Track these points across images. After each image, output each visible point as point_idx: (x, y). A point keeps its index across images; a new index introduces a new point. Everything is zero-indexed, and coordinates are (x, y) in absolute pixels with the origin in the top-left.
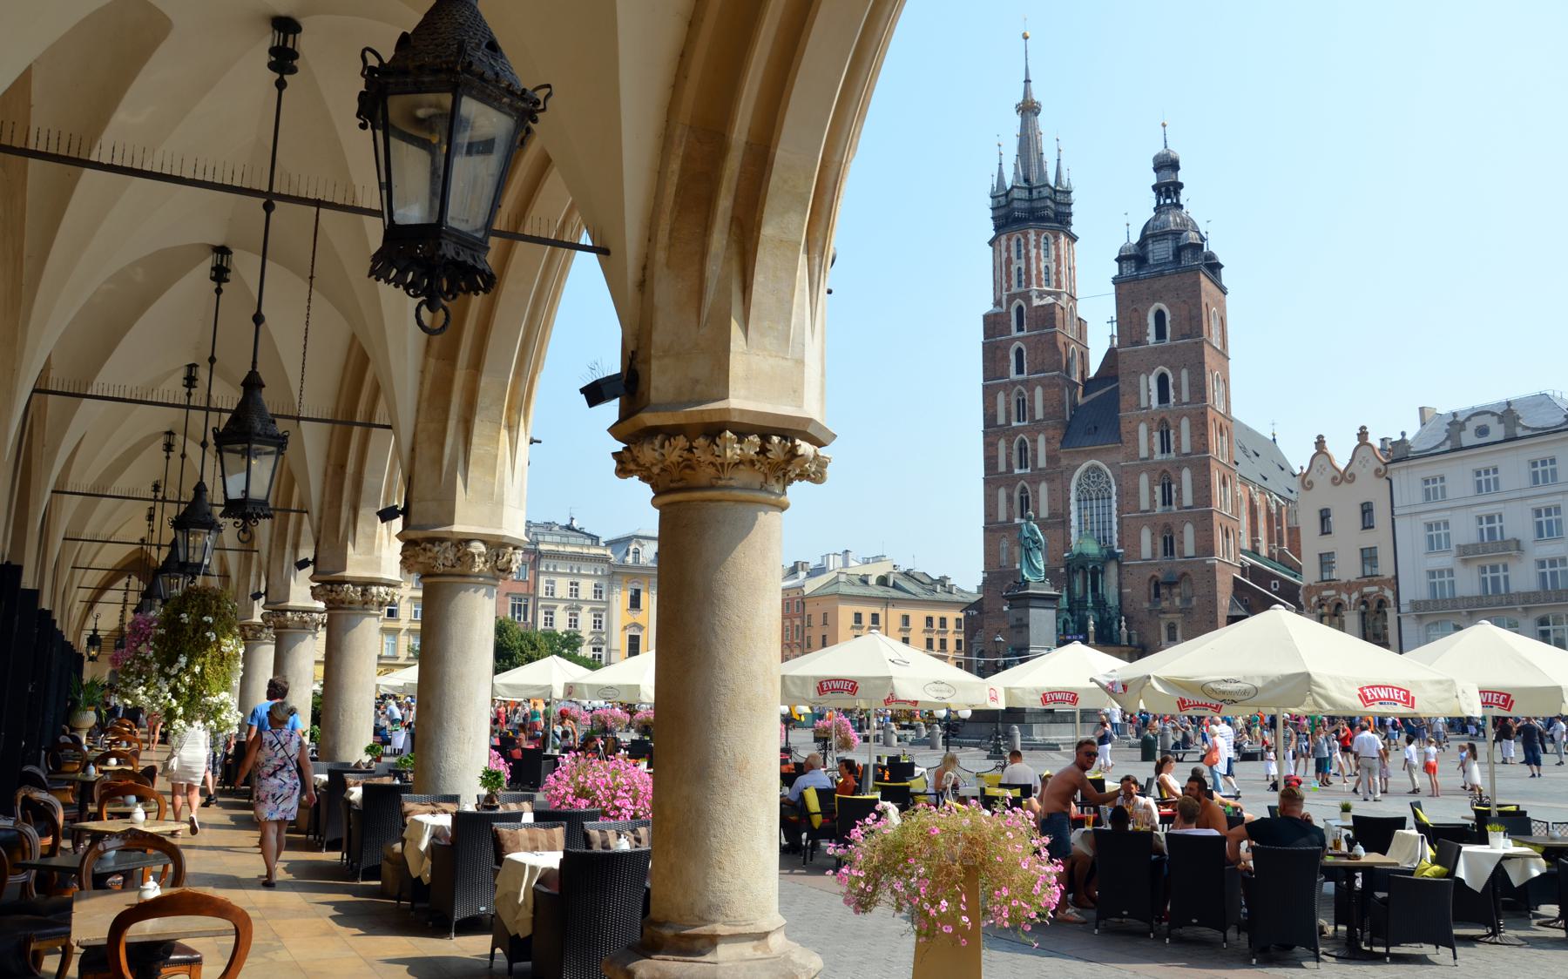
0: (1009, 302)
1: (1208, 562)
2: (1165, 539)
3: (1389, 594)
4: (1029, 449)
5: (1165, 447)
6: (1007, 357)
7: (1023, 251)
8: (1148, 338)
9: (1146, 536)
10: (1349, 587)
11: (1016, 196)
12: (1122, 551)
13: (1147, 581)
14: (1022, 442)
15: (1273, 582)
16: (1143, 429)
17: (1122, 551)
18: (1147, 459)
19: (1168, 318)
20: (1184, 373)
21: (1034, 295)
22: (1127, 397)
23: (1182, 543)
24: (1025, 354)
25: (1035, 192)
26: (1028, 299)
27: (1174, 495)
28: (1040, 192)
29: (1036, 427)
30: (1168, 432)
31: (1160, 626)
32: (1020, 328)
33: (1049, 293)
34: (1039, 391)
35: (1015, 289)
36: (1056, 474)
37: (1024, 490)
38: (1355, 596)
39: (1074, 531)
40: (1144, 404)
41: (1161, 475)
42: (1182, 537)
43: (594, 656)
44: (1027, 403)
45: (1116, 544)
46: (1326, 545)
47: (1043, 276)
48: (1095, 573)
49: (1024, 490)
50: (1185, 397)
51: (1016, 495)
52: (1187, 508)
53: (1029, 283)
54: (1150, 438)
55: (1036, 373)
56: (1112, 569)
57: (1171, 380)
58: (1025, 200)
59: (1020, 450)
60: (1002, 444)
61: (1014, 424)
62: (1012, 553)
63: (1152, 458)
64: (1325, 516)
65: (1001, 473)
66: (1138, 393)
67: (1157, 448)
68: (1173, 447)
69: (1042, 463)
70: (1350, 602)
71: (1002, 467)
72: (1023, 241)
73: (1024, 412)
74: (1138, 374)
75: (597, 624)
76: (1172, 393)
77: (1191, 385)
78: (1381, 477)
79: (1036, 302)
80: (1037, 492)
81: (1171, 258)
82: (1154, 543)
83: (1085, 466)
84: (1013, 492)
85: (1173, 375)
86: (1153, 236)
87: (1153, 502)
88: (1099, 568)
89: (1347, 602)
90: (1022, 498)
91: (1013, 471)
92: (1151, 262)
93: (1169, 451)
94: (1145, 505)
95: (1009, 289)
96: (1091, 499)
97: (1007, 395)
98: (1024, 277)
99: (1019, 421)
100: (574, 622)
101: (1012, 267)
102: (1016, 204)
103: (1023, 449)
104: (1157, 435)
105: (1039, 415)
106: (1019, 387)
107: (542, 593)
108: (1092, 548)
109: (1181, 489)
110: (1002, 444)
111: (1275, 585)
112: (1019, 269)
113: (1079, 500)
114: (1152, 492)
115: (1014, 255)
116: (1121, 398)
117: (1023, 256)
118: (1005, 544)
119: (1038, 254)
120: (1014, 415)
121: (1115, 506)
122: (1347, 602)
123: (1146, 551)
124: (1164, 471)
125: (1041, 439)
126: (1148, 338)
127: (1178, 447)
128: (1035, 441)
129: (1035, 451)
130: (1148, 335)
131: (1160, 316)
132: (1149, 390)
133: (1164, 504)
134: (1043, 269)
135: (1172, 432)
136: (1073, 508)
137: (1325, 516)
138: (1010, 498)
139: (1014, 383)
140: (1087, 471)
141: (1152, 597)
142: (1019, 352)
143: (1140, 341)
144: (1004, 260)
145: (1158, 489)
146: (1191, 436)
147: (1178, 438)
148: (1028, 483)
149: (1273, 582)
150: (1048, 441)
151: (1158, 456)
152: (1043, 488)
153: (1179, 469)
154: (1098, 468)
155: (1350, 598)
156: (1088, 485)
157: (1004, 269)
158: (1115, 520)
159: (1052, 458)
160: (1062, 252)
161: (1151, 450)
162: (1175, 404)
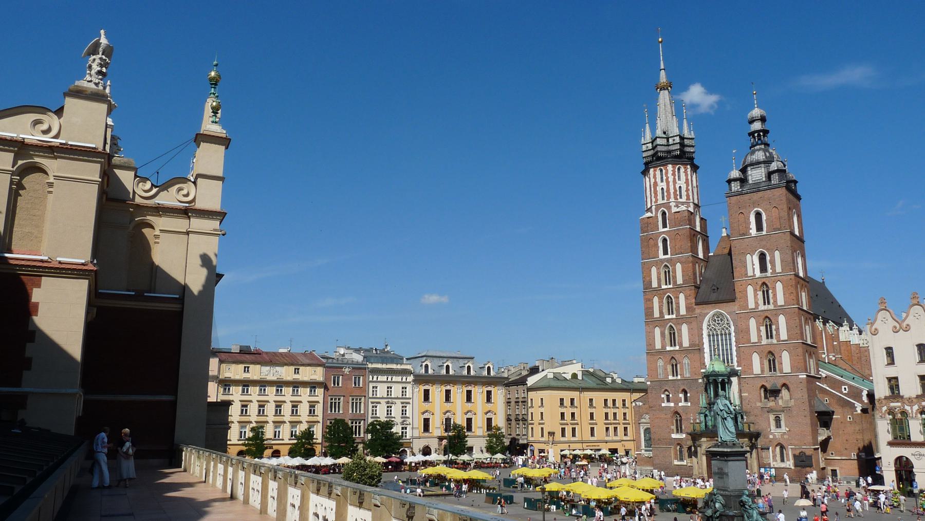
0: (657, 210)
1: (800, 376)
2: (770, 361)
4: (674, 303)
5: (766, 301)
6: (656, 245)
7: (664, 178)
8: (751, 231)
9: (756, 359)
10: (910, 401)
11: (658, 143)
12: (740, 368)
13: (759, 388)
15: (843, 387)
16: (750, 290)
17: (740, 368)
18: (754, 309)
19: (764, 217)
20: (777, 254)
21: (673, 204)
23: (782, 363)
24: (668, 243)
25: (671, 140)
26: (669, 208)
27: (774, 333)
28: (674, 140)
29: (678, 288)
30: (767, 291)
31: (769, 418)
32: (665, 226)
33: (683, 203)
34: (679, 267)
35: (660, 201)
36: (693, 320)
38: (916, 407)
39: (707, 356)
40: (750, 273)
41: (764, 319)
43: (402, 432)
44: (671, 273)
45: (735, 364)
46: (892, 372)
47: (678, 193)
48: (723, 384)
50: (779, 269)
51: (667, 332)
52: (783, 341)
53: (669, 198)
54: (756, 296)
56: (734, 380)
57: (768, 258)
58: (665, 145)
60: (656, 300)
61: (664, 287)
62: (666, 369)
63: (758, 309)
64: (889, 351)
65: (656, 318)
66: (746, 267)
67: (761, 301)
68: (771, 301)
69: (683, 311)
70: (912, 411)
71: (657, 314)
72: (664, 171)
73: (669, 279)
74: (745, 254)
75: (404, 412)
76: (769, 266)
77: (782, 261)
79: (674, 210)
80: (681, 330)
81: (764, 179)
82: (762, 364)
83: (712, 313)
84: (665, 330)
85: (770, 255)
86: (752, 164)
87: (760, 337)
88: (726, 380)
89: (910, 411)
90: (670, 333)
91: (664, 317)
92: (750, 182)
93: (769, 303)
94: (754, 338)
95: (656, 201)
97: (658, 269)
98: (665, 194)
99: (666, 284)
100: (389, 412)
101: (658, 187)
102: (659, 148)
104: (760, 294)
105: (680, 281)
107: (371, 395)
108: (719, 367)
109: (779, 328)
110: (656, 300)
111: (845, 388)
112: (662, 189)
113: (709, 336)
114: (759, 331)
115: (658, 180)
117: (664, 181)
118: (660, 363)
119: (674, 179)
120: (663, 281)
121: (733, 339)
123: (757, 369)
124: (767, 317)
125: (682, 296)
126: (751, 231)
127: (775, 301)
128: (677, 298)
129: (678, 304)
130: (751, 229)
131: (758, 216)
132: (753, 265)
133: (767, 338)
134: (678, 189)
135: (770, 291)
137: (889, 351)
138: (663, 334)
139: (662, 261)
141: (763, 399)
142: (665, 240)
143: (746, 232)
144: (652, 184)
145: (763, 329)
146: (784, 294)
147: (775, 295)
148: (674, 324)
149: (843, 387)
150: (686, 298)
151: (762, 307)
152: (685, 328)
153: (777, 315)
154: (721, 314)
155: (912, 409)
156: (714, 325)
157: (652, 189)
158: (734, 348)
159: (688, 308)
160: (689, 177)
161: (757, 303)
162: (772, 273)
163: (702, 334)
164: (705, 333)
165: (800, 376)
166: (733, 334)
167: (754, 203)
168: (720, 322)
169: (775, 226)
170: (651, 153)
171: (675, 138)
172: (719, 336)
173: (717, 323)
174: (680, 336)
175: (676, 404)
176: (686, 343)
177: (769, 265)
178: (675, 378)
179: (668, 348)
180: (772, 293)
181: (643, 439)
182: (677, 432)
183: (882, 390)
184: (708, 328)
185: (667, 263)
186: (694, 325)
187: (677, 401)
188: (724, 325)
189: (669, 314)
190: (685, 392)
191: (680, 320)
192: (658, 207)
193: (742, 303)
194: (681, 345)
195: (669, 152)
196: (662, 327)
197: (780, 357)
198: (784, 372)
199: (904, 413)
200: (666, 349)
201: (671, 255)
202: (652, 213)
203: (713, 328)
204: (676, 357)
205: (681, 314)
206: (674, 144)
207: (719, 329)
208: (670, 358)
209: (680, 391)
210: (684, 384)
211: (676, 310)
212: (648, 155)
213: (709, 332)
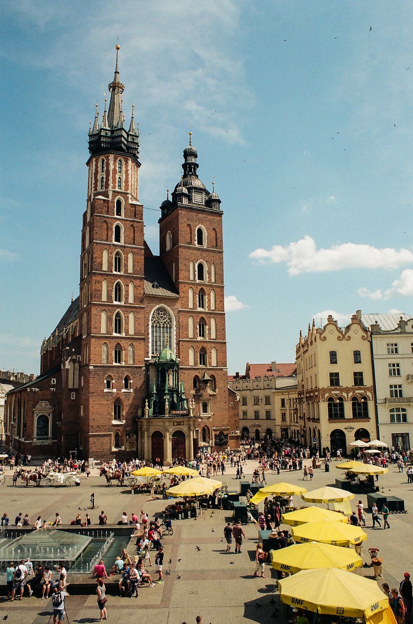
2: (200, 355)
3: (369, 394)
9: (191, 353)
14: (118, 284)
22: (183, 272)
23: (211, 358)
24: (122, 231)
37: (118, 315)
42: (211, 355)
49: (118, 315)
50: (213, 281)
52: (213, 339)
66: (189, 271)
67: (198, 304)
68: (207, 305)
69: (131, 300)
74: (189, 260)
78: (342, 340)
83: (158, 306)
91: (112, 302)
96: (160, 327)
97: (110, 253)
103: (118, 288)
106: (119, 249)
113: (153, 327)
116: (180, 271)
122: (346, 397)
127: (209, 306)
128: (128, 286)
129: (127, 292)
136: (150, 331)
138: (109, 319)
140: (158, 309)
145: (198, 326)
148: (123, 311)
150: (135, 287)
154: (164, 310)
156: (158, 318)
163: (148, 325)
164: (150, 323)
165: (224, 370)
166: (174, 328)
167: (199, 220)
168: (163, 315)
169: (213, 244)
172: (162, 328)
173: (161, 317)
174: (127, 324)
175: (119, 389)
176: (131, 332)
177: (207, 274)
178: (118, 364)
179: (115, 334)
180: (207, 298)
181: (36, 427)
182: (115, 419)
183: (324, 382)
184: (152, 320)
185: (121, 250)
186: (141, 316)
187: (119, 389)
188: (166, 319)
189: (116, 300)
190: (127, 379)
191: (128, 308)
193: (184, 302)
194: (127, 332)
197: (211, 353)
198: (212, 366)
199: (341, 399)
200: (112, 334)
201: (125, 243)
203: (156, 320)
204: (123, 343)
205: (129, 302)
207: (162, 323)
208: (116, 344)
209: (124, 377)
210: (128, 371)
211: (125, 297)
213: (153, 324)
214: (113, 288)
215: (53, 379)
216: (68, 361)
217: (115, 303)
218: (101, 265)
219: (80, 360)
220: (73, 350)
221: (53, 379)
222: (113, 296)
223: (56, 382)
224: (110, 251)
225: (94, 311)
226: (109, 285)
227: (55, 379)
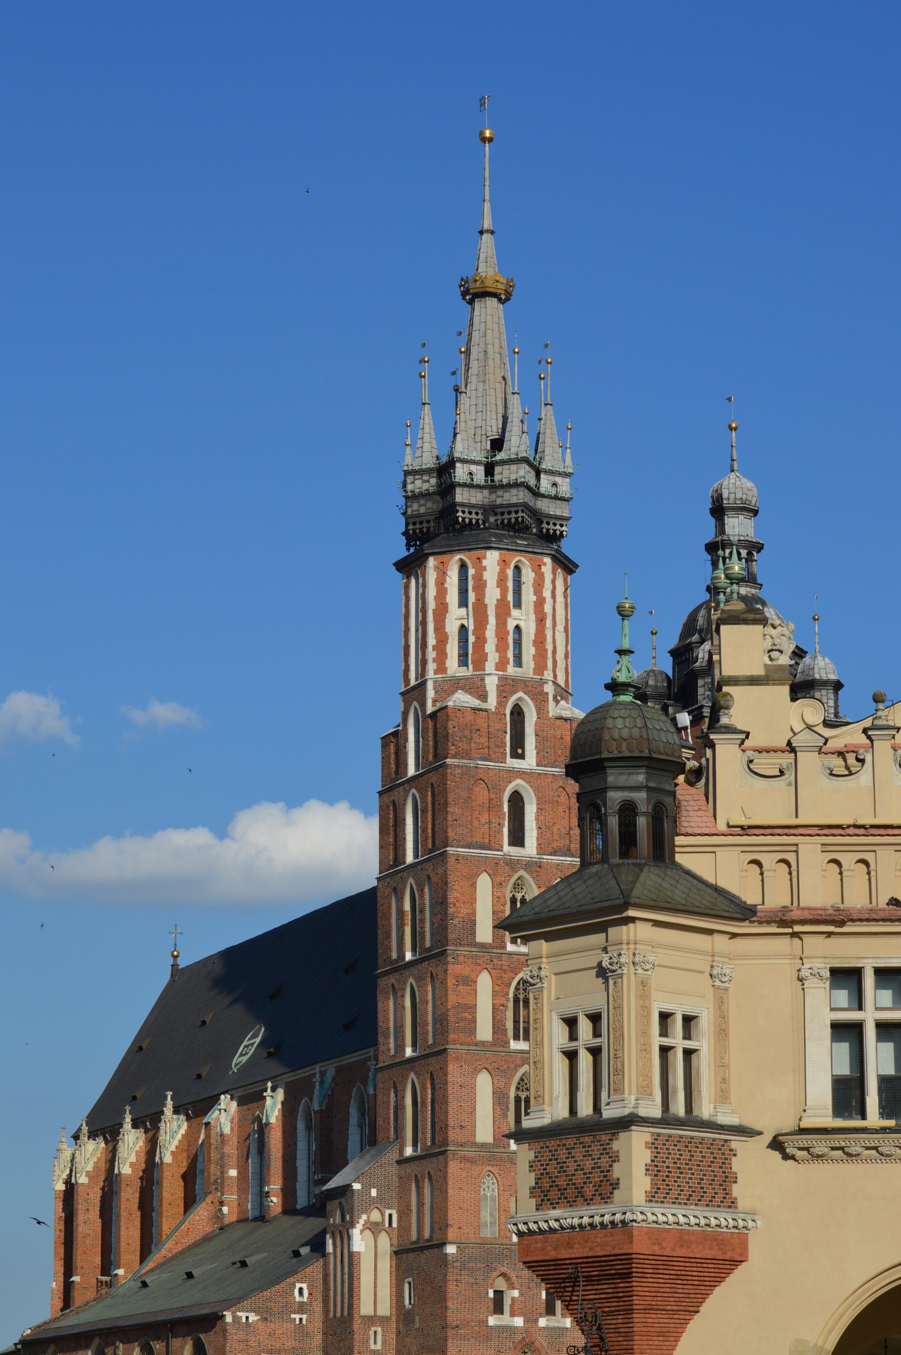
21: (549, 688)
26: (540, 699)
35: (511, 670)
55: (554, 853)
59: (516, 1000)
79: (553, 710)
84: (508, 1085)
91: (508, 1043)
97: (497, 886)
106: (522, 873)
138: (499, 1097)
139: (513, 864)
170: (478, 497)
171: (559, 480)
185: (530, 873)
189: (516, 1037)
192: (507, 686)
195: (538, 517)
196: (499, 1072)
201: (541, 850)
202: (484, 697)
206: (556, 498)
212: (473, 501)
214: (508, 1000)
215: (298, 1285)
216: (359, 1226)
217: (514, 1045)
218: (471, 924)
219: (395, 1225)
220: (374, 1192)
221: (298, 1285)
222: (510, 1025)
223: (310, 1294)
224: (499, 879)
225: (455, 1073)
226: (497, 988)
227: (304, 1286)
